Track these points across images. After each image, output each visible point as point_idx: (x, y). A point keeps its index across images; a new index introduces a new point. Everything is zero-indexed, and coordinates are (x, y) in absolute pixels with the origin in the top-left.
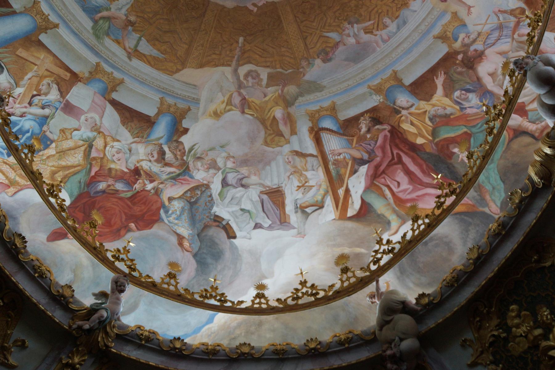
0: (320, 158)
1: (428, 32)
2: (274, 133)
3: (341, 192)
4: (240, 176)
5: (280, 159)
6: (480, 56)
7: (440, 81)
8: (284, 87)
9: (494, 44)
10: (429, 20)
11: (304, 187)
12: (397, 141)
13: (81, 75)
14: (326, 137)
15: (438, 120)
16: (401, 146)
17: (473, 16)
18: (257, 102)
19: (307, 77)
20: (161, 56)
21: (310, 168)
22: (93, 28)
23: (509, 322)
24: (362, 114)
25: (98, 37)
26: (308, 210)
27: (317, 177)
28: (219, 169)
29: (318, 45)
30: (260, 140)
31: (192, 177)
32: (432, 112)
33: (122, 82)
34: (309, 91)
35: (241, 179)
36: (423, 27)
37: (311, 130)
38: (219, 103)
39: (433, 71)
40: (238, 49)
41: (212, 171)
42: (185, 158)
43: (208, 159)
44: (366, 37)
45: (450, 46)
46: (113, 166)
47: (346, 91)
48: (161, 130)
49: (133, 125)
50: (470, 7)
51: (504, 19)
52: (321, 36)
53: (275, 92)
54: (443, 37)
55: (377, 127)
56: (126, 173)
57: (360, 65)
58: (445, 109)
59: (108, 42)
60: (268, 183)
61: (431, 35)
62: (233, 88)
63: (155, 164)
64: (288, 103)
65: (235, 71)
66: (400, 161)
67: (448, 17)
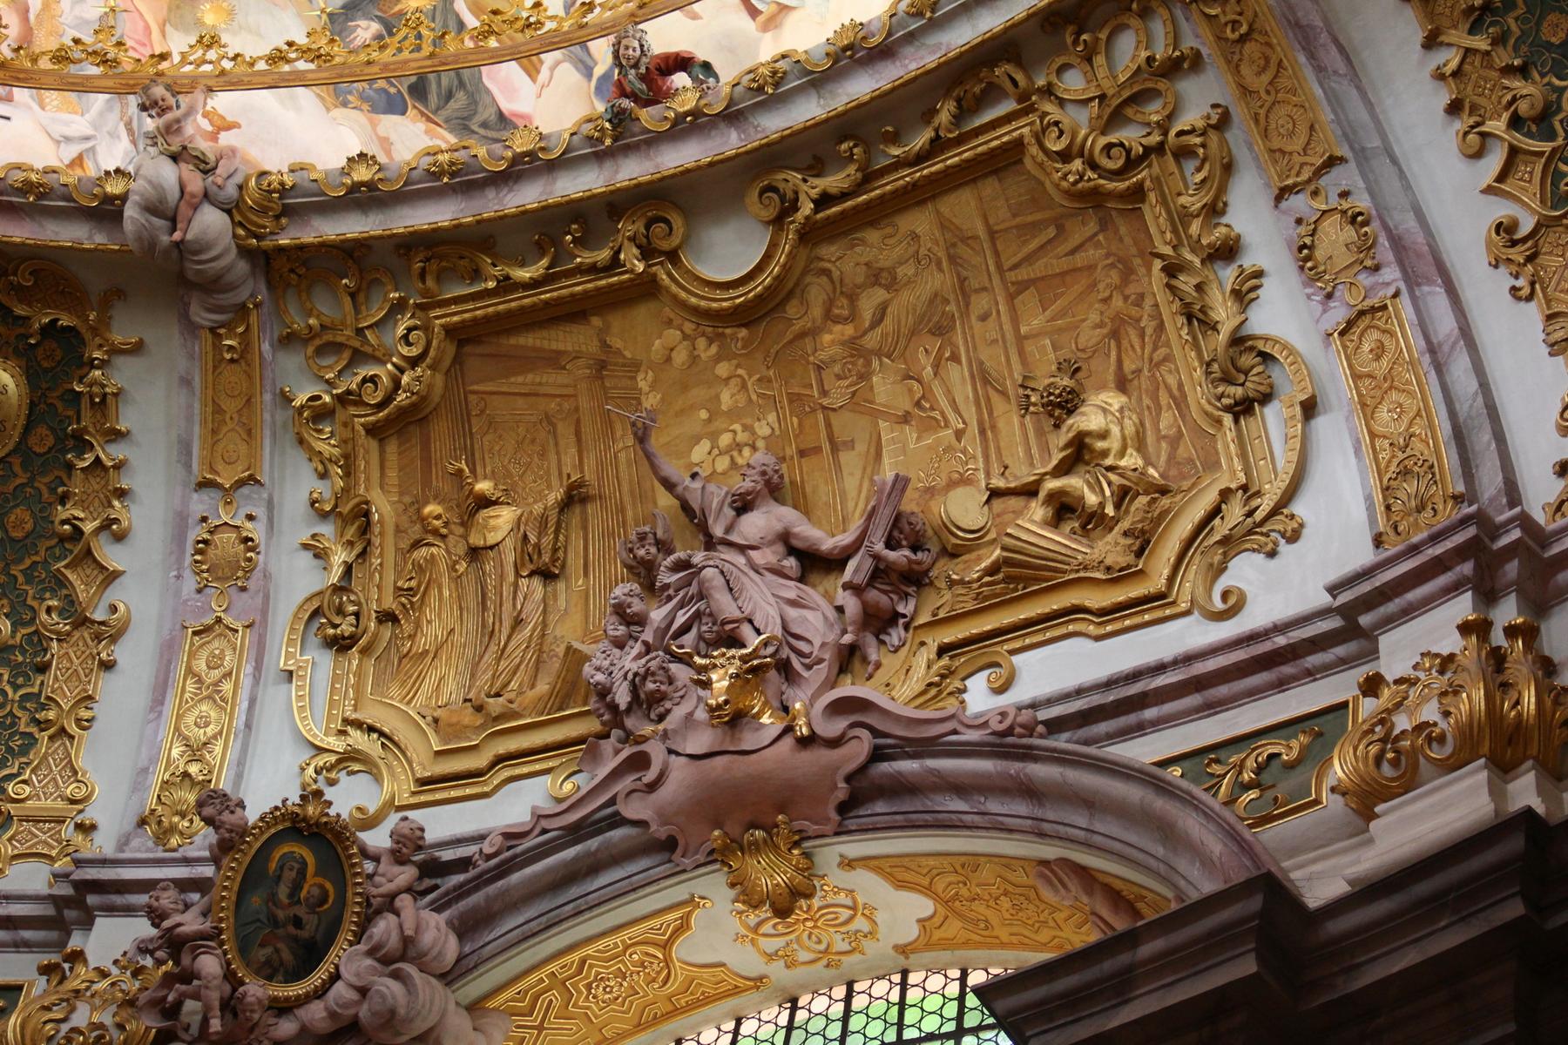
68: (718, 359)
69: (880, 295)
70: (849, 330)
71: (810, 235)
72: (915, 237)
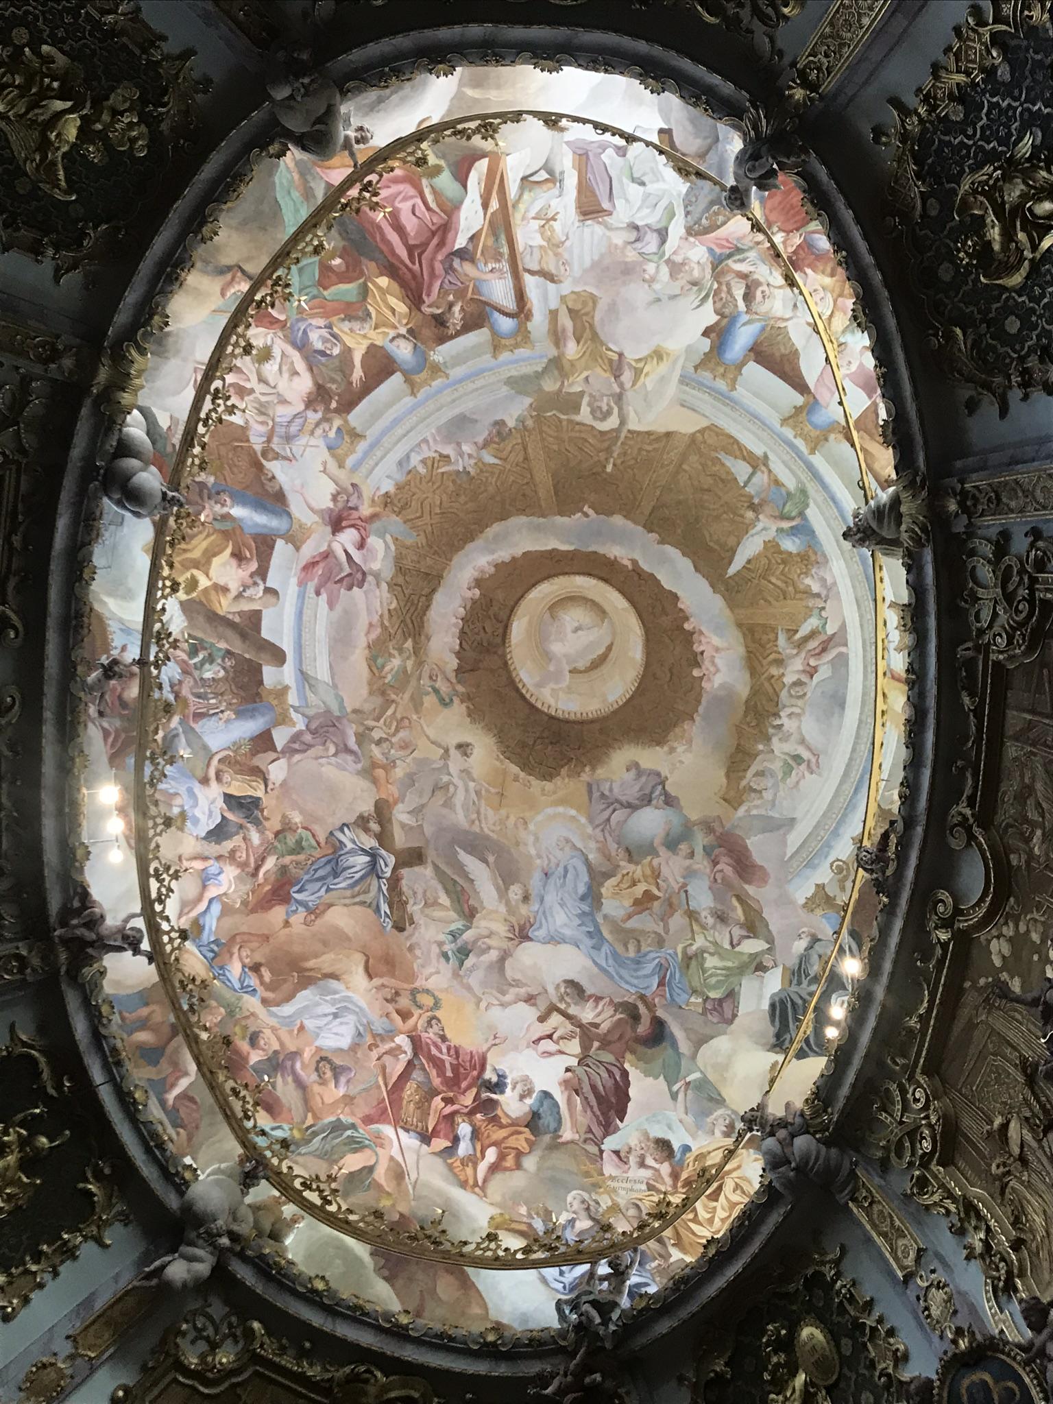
0: (521, 268)
1: (372, 446)
2: (581, 318)
3: (494, 205)
4: (638, 245)
5: (577, 270)
6: (310, 403)
7: (358, 373)
8: (560, 390)
9: (295, 416)
10: (372, 463)
11: (547, 219)
12: (413, 284)
13: (841, 437)
14: (510, 304)
15: (360, 314)
16: (408, 276)
17: (320, 460)
18: (599, 370)
19: (528, 401)
20: (722, 456)
21: (535, 250)
22: (807, 505)
23: (143, 128)
24: (458, 334)
25: (803, 492)
26: (543, 175)
27: (527, 235)
28: (668, 261)
29: (509, 448)
30: (602, 306)
31: (711, 250)
32: (367, 326)
33: (784, 421)
34: (525, 378)
35: (637, 240)
36: (379, 454)
37: (529, 316)
38: (655, 373)
39: (368, 388)
40: (615, 455)
41: (678, 259)
42: (716, 286)
43: (682, 281)
44: (448, 450)
45: (346, 421)
46: (828, 281)
47: (478, 373)
48: (743, 337)
49: (783, 351)
50: (324, 471)
51: (284, 449)
52: (505, 460)
53: (573, 383)
54: (356, 436)
55: (439, 311)
56: (809, 266)
57: (457, 411)
58: (351, 330)
59: (790, 484)
60: (598, 230)
61: (369, 440)
62: (629, 395)
63: (762, 280)
64: (556, 365)
65: (623, 422)
66: (410, 249)
67: (350, 461)
68: (1017, 926)
69: (1030, 802)
70: (1039, 832)
71: (985, 818)
72: (1016, 759)
